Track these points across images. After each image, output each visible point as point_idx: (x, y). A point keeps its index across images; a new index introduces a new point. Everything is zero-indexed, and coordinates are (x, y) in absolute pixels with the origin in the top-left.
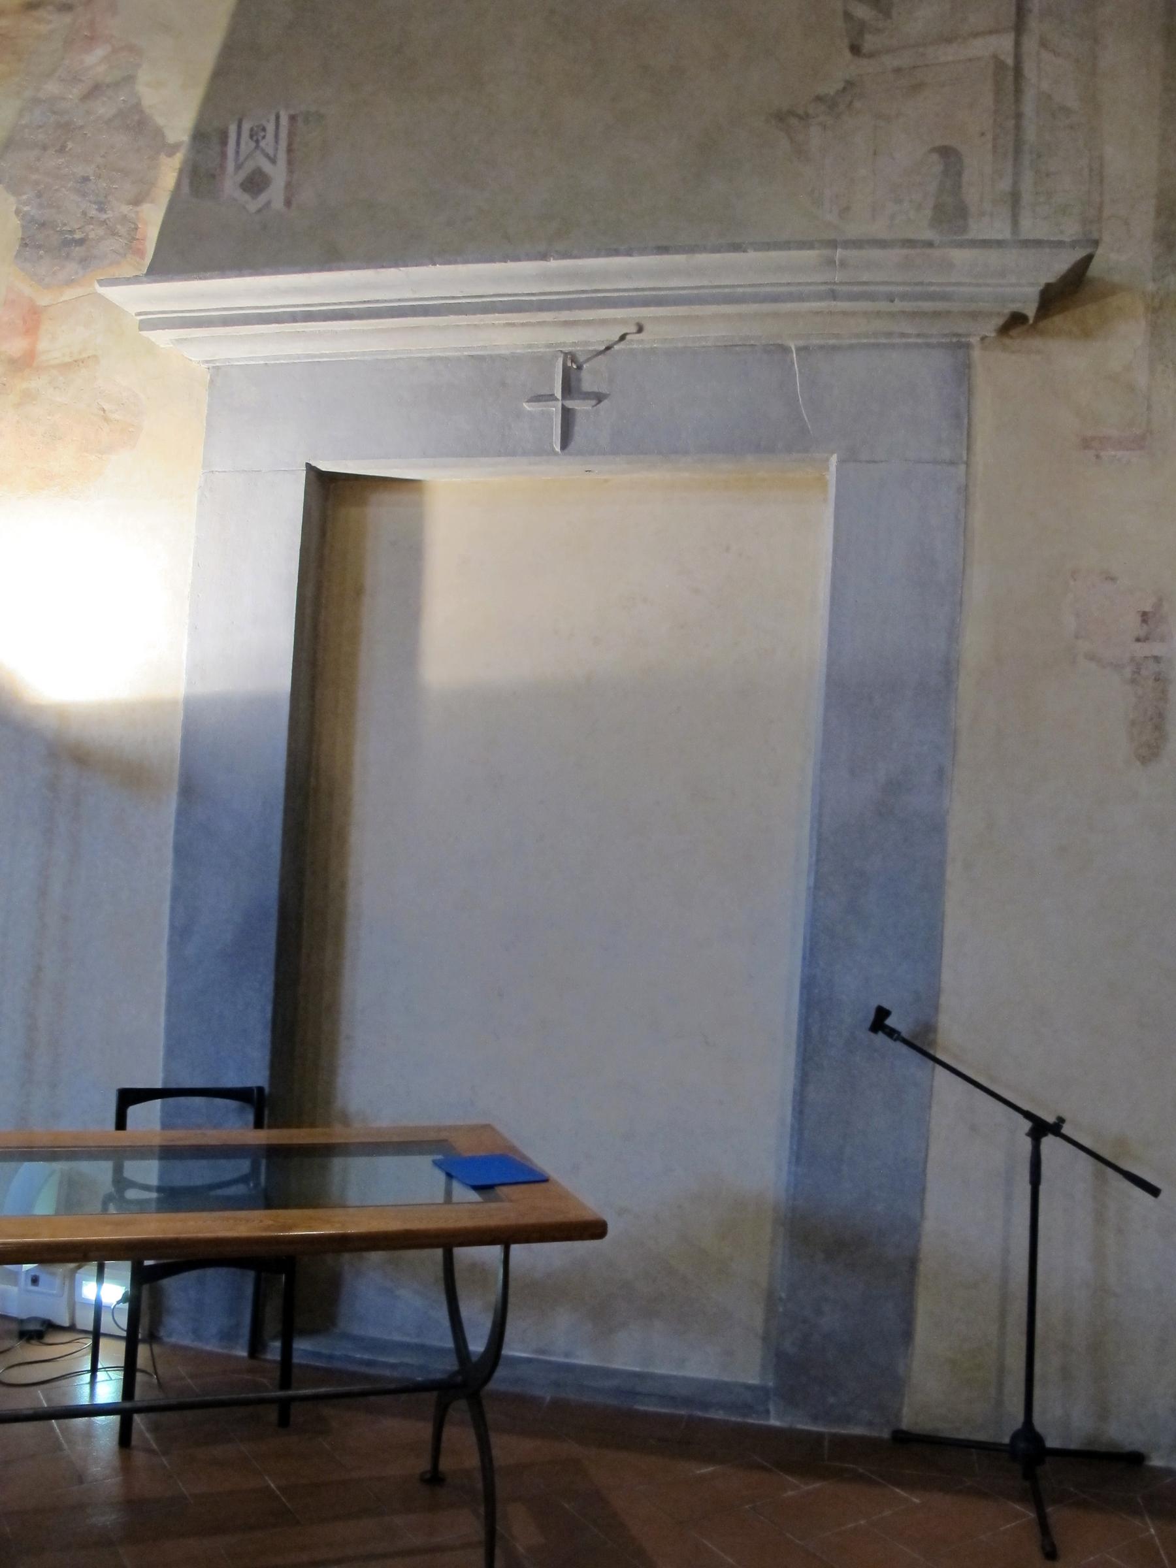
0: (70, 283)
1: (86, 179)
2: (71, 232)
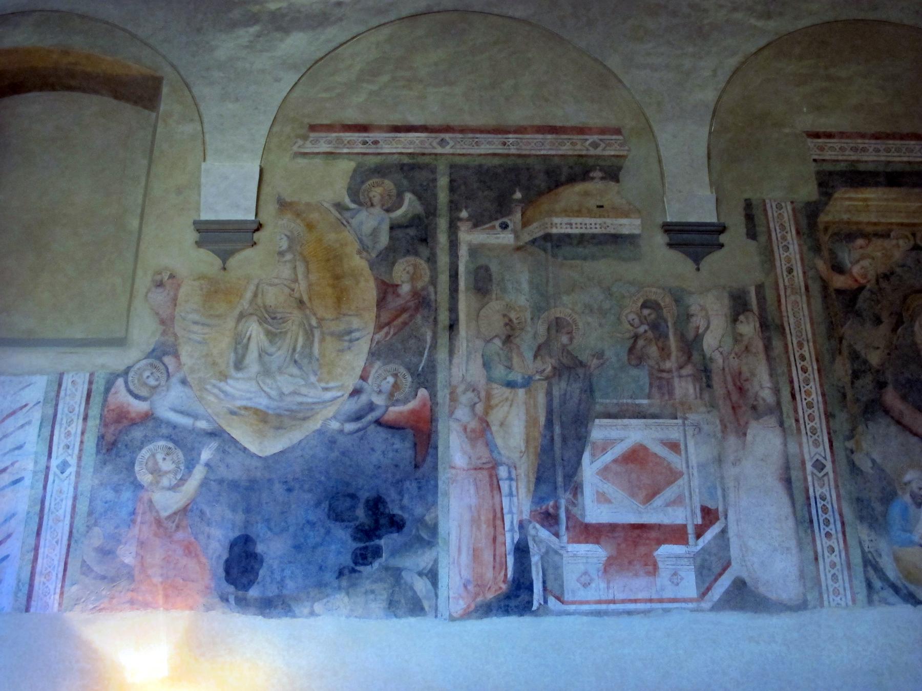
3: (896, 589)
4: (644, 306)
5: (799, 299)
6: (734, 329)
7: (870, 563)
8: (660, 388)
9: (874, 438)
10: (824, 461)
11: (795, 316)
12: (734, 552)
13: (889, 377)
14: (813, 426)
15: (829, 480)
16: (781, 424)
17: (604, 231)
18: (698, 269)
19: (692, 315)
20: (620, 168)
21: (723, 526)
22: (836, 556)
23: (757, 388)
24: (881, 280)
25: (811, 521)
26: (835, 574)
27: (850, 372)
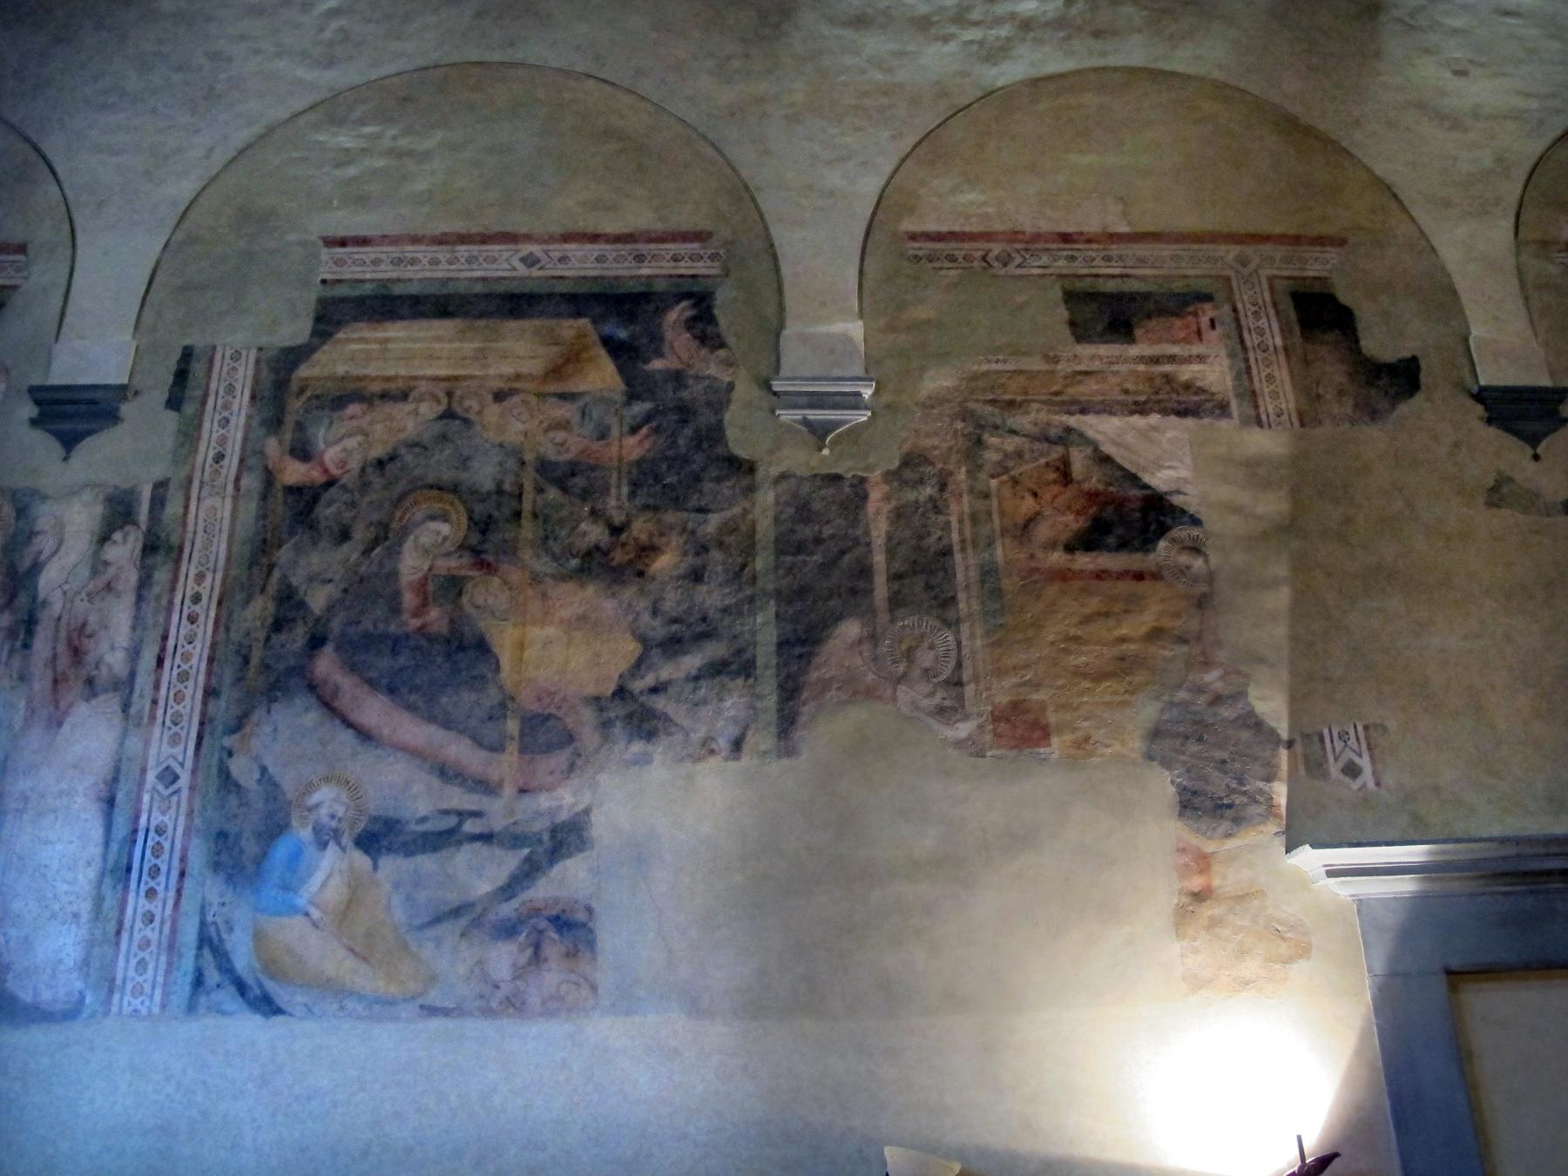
0: (1228, 835)
1: (1224, 762)
2: (1221, 798)
3: (241, 988)
6: (96, 554)
7: (209, 942)
9: (275, 730)
10: (178, 770)
11: (205, 532)
13: (336, 625)
14: (177, 711)
15: (179, 803)
16: (126, 707)
19: (38, 533)
22: (153, 929)
24: (369, 470)
25: (129, 869)
26: (143, 959)
27: (270, 620)
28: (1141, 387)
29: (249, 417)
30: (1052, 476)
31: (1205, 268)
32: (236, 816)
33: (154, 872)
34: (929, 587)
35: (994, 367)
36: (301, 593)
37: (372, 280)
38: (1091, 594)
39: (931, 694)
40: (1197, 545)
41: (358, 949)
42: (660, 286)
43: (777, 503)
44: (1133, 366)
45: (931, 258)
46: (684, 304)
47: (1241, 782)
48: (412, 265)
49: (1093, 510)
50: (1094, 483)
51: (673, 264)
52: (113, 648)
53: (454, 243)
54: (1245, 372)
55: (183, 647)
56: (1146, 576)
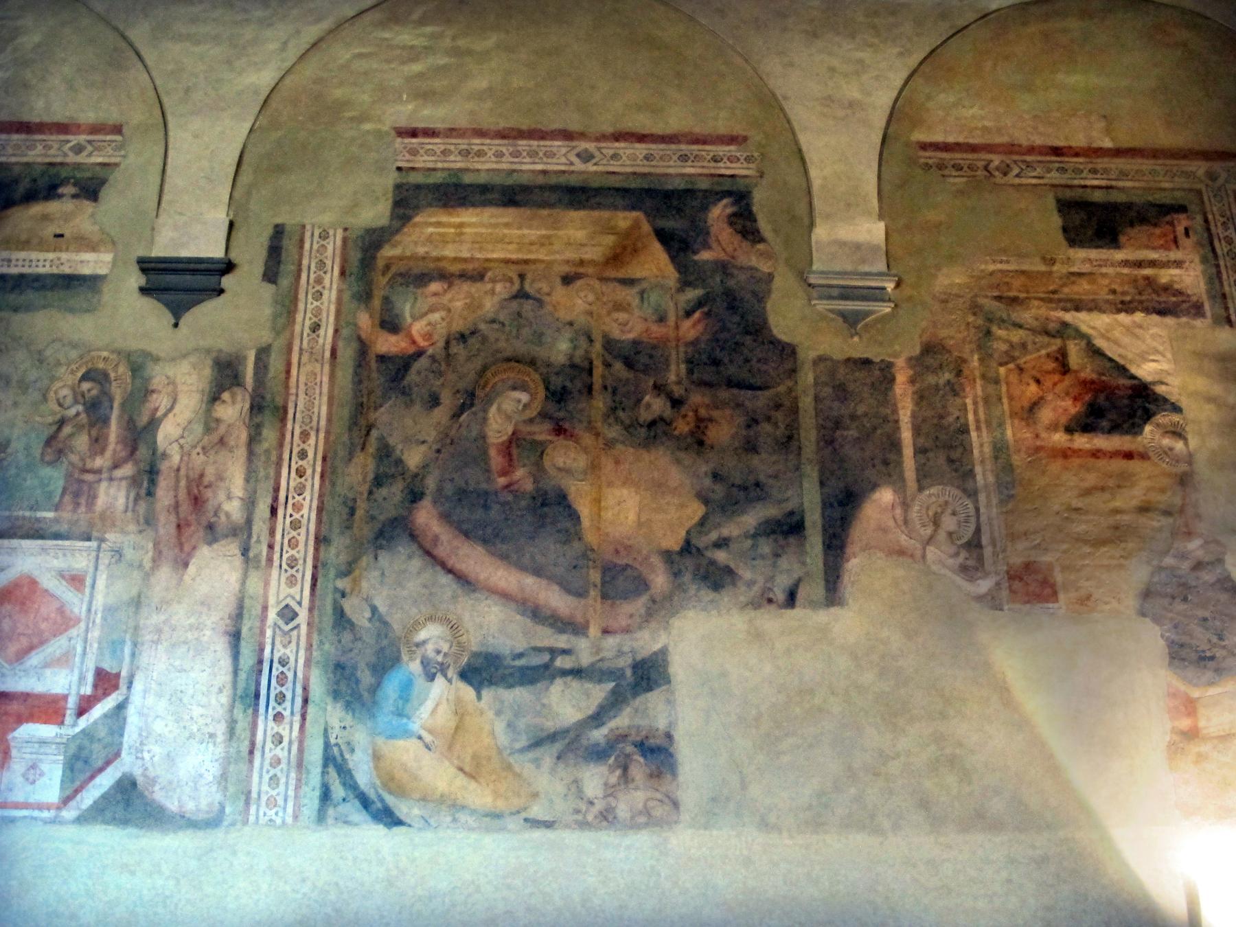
0: (1211, 684)
1: (1205, 619)
2: (1204, 651)
3: (365, 802)
4: (85, 378)
5: (318, 370)
6: (209, 411)
7: (334, 761)
8: (77, 495)
9: (383, 574)
10: (297, 608)
12: (130, 736)
13: (431, 483)
16: (245, 551)
17: (55, 271)
18: (176, 325)
19: (153, 391)
20: (103, 182)
21: (121, 698)
22: (282, 749)
23: (222, 496)
25: (257, 696)
26: (275, 775)
27: (371, 476)
28: (1126, 288)
29: (340, 291)
30: (1051, 365)
31: (1180, 182)
32: (351, 650)
33: (281, 698)
34: (951, 461)
35: (1000, 266)
36: (398, 452)
37: (443, 169)
38: (1088, 470)
39: (957, 554)
40: (1179, 430)
41: (467, 769)
42: (704, 185)
43: (816, 384)
44: (1118, 269)
45: (941, 166)
46: (725, 201)
47: (1221, 638)
48: (478, 156)
49: (1088, 397)
50: (1088, 373)
51: (712, 164)
52: (229, 498)
53: (515, 138)
54: (1215, 278)
55: (294, 498)
56: (1135, 456)
